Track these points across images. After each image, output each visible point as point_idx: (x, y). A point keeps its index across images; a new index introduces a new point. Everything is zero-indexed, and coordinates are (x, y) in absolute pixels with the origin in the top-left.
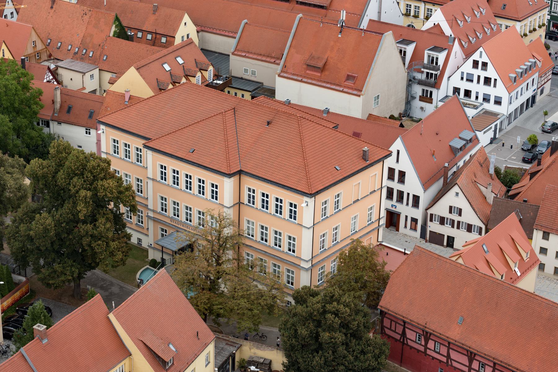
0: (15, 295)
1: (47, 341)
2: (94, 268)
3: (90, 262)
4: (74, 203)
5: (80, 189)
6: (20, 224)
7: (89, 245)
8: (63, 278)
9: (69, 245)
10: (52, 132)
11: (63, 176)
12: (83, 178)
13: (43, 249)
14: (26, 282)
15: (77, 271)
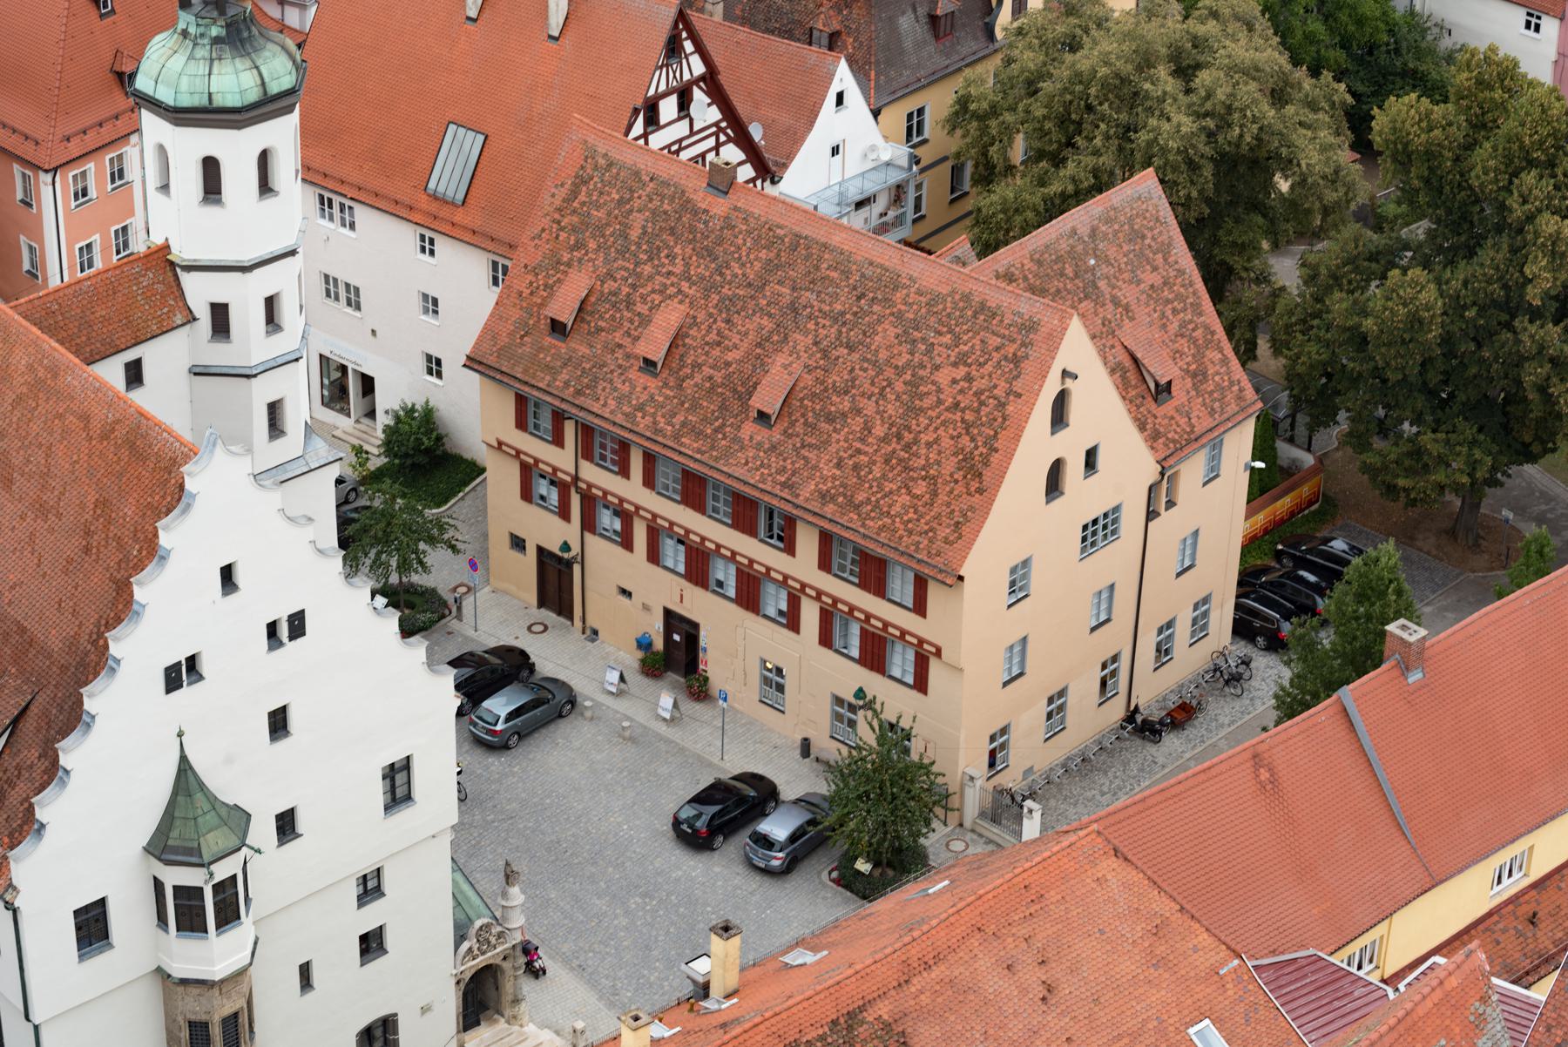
0: (1279, 503)
1: (1420, 675)
2: (1532, 458)
3: (1527, 438)
4: (1514, 251)
5: (1540, 211)
6: (1328, 290)
7: (1542, 389)
8: (1440, 476)
9: (1475, 377)
10: (1418, 8)
11: (1492, 163)
12: (1555, 176)
13: (1393, 377)
14: (1314, 471)
15: (1489, 460)
